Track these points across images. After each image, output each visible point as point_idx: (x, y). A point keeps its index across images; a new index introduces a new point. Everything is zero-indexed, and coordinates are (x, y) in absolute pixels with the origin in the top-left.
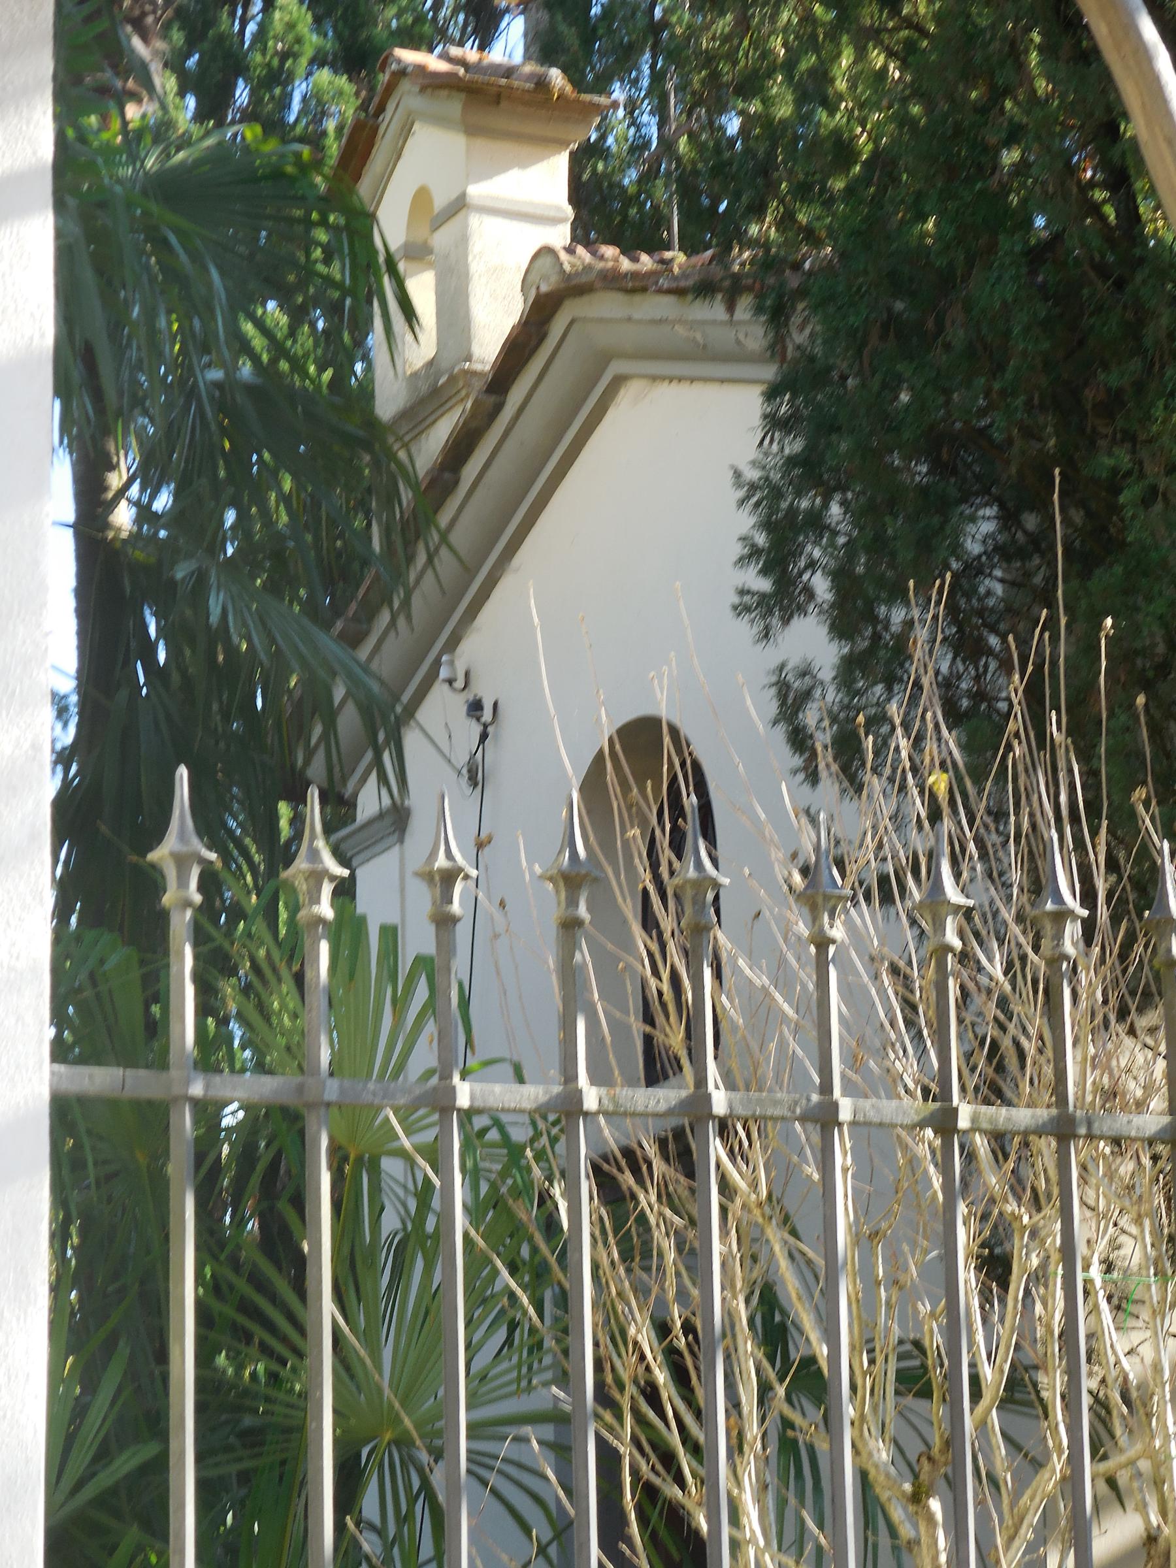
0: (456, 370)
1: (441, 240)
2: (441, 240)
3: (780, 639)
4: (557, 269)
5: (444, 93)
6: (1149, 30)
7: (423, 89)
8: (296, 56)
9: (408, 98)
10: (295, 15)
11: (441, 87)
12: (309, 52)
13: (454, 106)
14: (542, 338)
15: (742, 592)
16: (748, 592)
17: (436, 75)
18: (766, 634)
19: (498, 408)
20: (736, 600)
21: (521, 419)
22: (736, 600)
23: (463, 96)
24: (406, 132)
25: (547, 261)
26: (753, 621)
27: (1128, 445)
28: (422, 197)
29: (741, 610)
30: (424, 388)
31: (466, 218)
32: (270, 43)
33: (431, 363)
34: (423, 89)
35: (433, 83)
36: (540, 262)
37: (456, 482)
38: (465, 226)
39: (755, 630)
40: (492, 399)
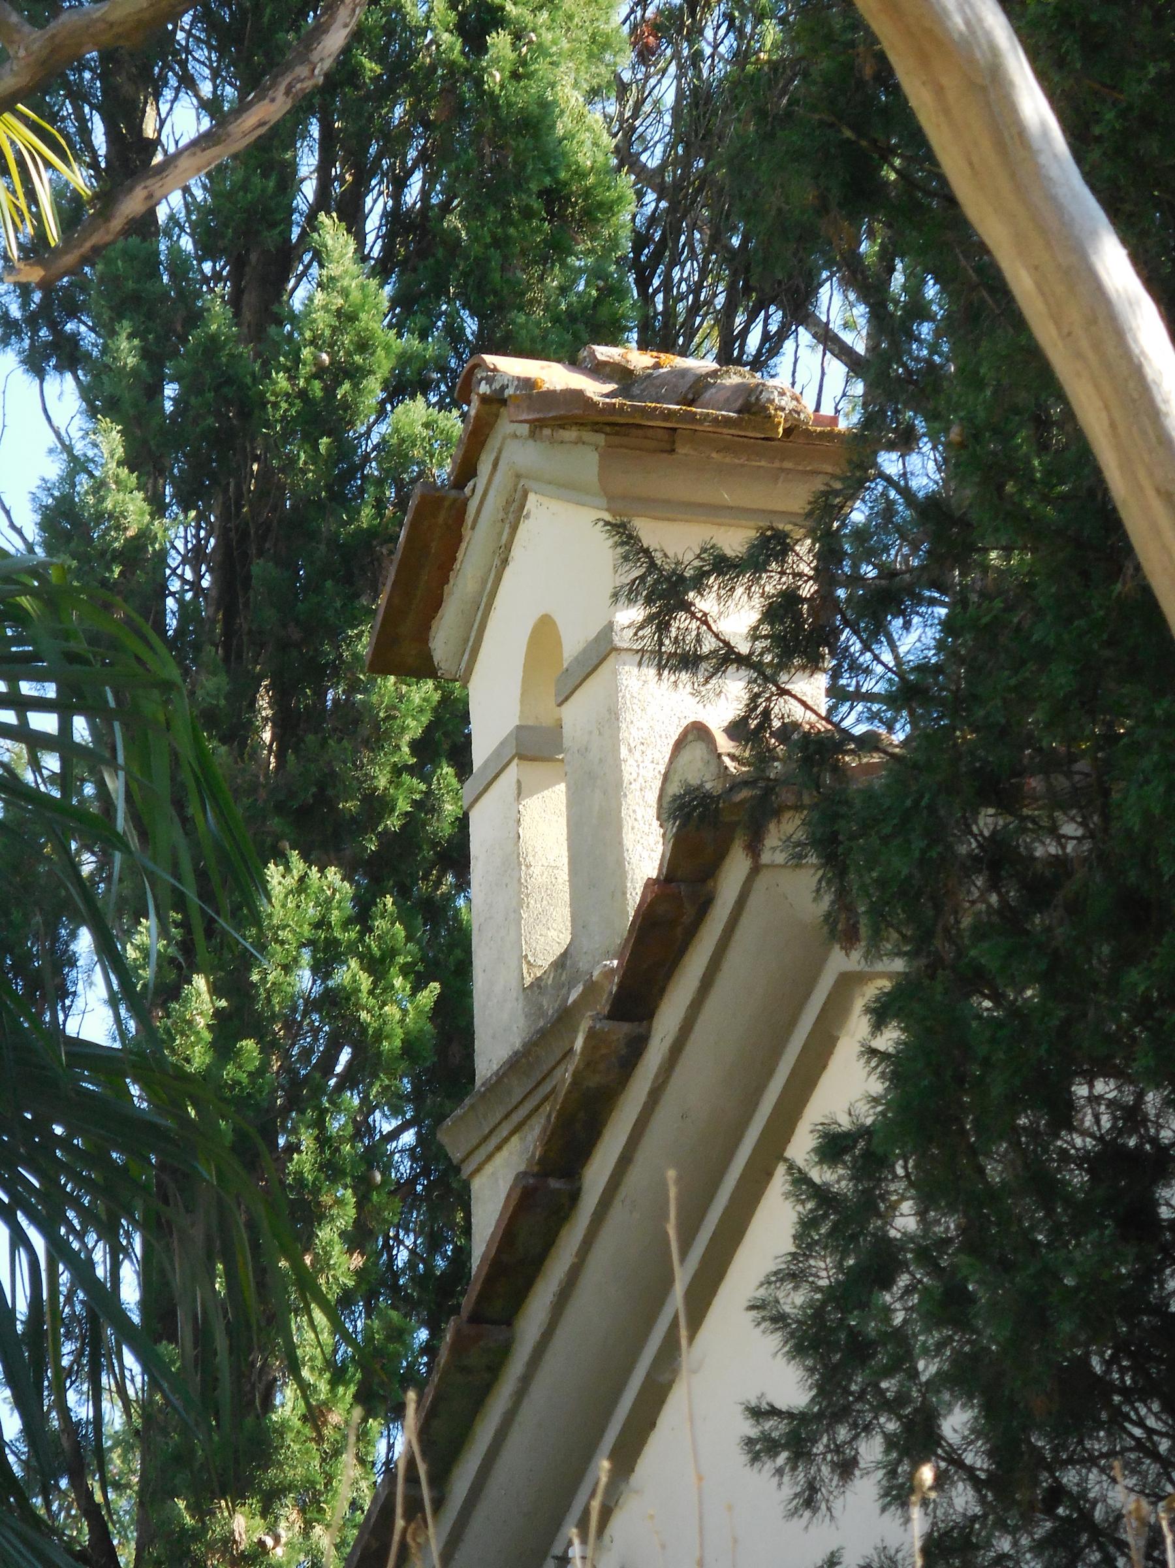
0: (596, 974)
1: (576, 717)
2: (576, 717)
3: (837, 1505)
4: (713, 768)
5: (571, 434)
6: (1114, 265)
7: (537, 426)
8: (355, 374)
9: (514, 450)
10: (356, 296)
11: (562, 423)
12: (383, 365)
13: (584, 458)
14: (705, 905)
15: (757, 1413)
16: (773, 1412)
17: (552, 398)
18: (809, 1499)
19: (637, 1046)
20: (750, 1429)
21: (678, 1069)
22: (750, 1429)
23: (600, 439)
24: (514, 513)
25: (696, 752)
26: (780, 1472)
27: (350, 1129)
28: (544, 632)
29: (760, 1449)
30: (550, 1006)
31: (615, 673)
32: (306, 353)
33: (561, 963)
34: (537, 426)
35: (559, 415)
36: (686, 756)
37: (575, 1196)
38: (614, 689)
39: (788, 1490)
40: (625, 1028)
